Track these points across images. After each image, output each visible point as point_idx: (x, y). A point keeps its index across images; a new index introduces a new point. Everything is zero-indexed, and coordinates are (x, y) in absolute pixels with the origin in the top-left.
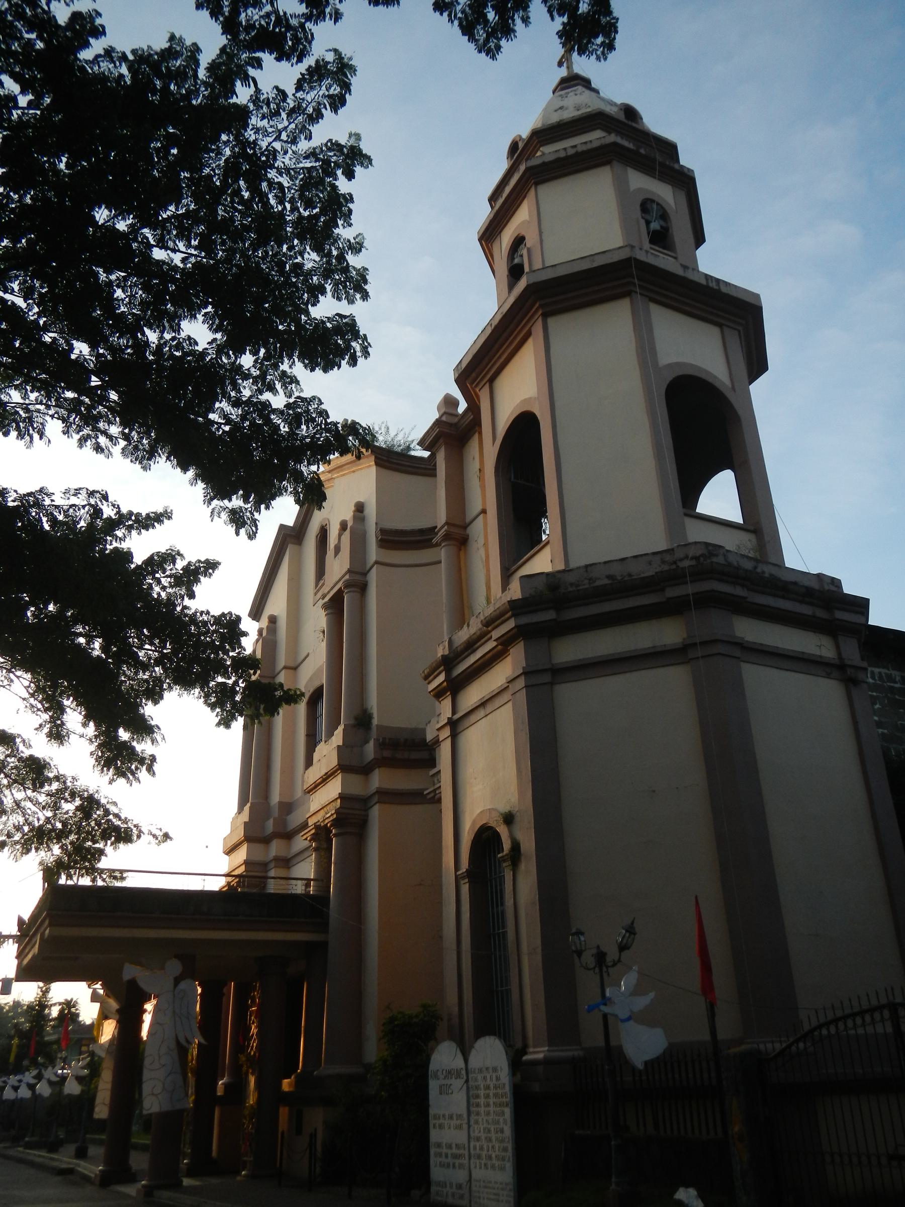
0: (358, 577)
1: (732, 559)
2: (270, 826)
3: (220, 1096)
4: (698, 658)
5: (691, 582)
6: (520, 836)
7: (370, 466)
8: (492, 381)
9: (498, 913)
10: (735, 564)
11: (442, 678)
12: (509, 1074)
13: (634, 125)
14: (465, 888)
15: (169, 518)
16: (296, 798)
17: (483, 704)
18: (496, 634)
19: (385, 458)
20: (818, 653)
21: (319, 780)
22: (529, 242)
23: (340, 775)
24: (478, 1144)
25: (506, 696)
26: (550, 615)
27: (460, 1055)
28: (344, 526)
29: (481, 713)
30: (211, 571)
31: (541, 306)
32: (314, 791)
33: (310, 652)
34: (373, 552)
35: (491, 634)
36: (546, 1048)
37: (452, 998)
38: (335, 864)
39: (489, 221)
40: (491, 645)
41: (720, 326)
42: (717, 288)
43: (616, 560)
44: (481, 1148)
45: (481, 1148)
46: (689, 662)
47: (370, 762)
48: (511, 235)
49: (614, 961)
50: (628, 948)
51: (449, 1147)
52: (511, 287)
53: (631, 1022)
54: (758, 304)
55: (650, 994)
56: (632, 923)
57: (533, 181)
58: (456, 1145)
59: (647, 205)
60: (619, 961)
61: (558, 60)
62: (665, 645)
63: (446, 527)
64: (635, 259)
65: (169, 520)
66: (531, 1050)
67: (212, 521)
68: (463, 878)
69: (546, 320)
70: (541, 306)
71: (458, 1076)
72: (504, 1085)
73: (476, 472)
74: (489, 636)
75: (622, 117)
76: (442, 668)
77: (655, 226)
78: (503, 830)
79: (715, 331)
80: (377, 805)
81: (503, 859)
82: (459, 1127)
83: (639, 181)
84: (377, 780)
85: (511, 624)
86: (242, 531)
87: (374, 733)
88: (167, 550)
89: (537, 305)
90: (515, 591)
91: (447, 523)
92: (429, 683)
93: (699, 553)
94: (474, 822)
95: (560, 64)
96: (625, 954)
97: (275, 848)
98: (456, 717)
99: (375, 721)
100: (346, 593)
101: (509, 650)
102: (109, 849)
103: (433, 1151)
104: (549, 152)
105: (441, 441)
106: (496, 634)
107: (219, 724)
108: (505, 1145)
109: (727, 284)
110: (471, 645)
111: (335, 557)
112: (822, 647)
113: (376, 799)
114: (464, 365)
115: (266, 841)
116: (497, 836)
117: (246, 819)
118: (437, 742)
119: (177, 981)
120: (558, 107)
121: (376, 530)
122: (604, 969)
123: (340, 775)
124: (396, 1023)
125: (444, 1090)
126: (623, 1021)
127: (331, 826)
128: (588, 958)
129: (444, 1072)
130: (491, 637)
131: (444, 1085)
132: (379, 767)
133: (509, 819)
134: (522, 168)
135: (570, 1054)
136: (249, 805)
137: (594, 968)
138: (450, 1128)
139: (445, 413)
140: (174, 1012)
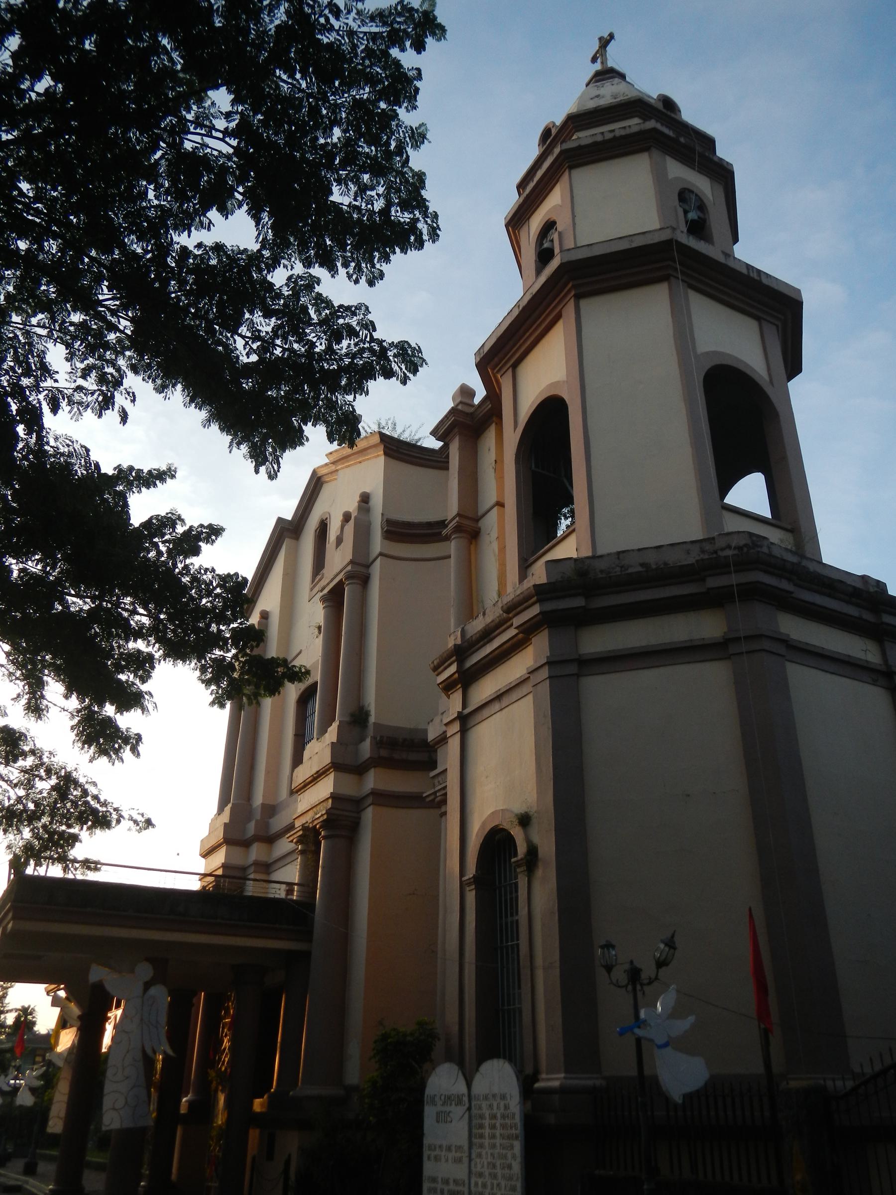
0: (359, 569)
1: (776, 552)
2: (251, 829)
3: (183, 1114)
4: (742, 653)
5: (736, 572)
6: (536, 839)
7: (378, 456)
8: (515, 366)
10: (779, 556)
11: (453, 669)
12: (520, 1103)
13: (673, 115)
14: (471, 897)
15: (173, 477)
16: (281, 800)
17: (499, 697)
18: (517, 621)
19: (395, 448)
20: (863, 657)
21: (310, 779)
22: (560, 226)
23: (333, 773)
24: (480, 1181)
25: (525, 689)
27: (461, 1077)
28: (347, 517)
29: (496, 706)
30: (214, 537)
32: (302, 791)
33: (303, 649)
34: (377, 543)
35: (511, 621)
36: (562, 1075)
37: (452, 1017)
38: (323, 867)
39: (517, 206)
40: (512, 632)
41: (758, 319)
42: (758, 279)
43: (651, 548)
44: (484, 1185)
45: (484, 1185)
46: (729, 658)
47: (365, 762)
48: (542, 220)
49: (650, 978)
50: (667, 965)
51: (446, 1182)
52: (539, 272)
53: (669, 1050)
54: (799, 299)
55: (689, 1018)
56: (673, 936)
58: (454, 1181)
59: (685, 195)
60: (656, 978)
61: (592, 56)
63: (457, 519)
64: (677, 241)
65: (172, 479)
66: (544, 1076)
67: (230, 452)
68: (469, 884)
69: (579, 303)
70: (574, 287)
71: (459, 1102)
72: (514, 1114)
73: (491, 464)
74: (509, 624)
75: (660, 106)
76: (454, 658)
77: (692, 215)
78: (517, 833)
79: (753, 324)
80: (372, 806)
81: (518, 864)
82: (459, 1161)
83: (677, 171)
84: (372, 781)
85: (535, 610)
86: (263, 469)
87: (371, 731)
88: (167, 514)
89: (570, 285)
90: (539, 574)
91: (458, 515)
92: (438, 675)
93: (742, 543)
94: (484, 824)
95: (594, 60)
96: (663, 971)
97: (256, 852)
98: (466, 711)
99: (372, 719)
100: (348, 584)
101: (531, 639)
102: (84, 834)
103: (426, 1186)
104: (584, 137)
105: (456, 430)
106: (517, 621)
107: (213, 703)
108: (513, 1183)
109: (767, 275)
110: (487, 635)
112: (868, 651)
113: (370, 800)
114: (486, 349)
115: (246, 844)
116: (510, 840)
117: (227, 820)
118: (443, 739)
119: (147, 986)
120: (593, 96)
121: (382, 520)
122: (638, 987)
123: (333, 773)
124: (389, 1041)
125: (442, 1117)
126: (661, 1047)
127: (320, 827)
128: (620, 974)
129: (443, 1098)
130: (512, 625)
131: (442, 1112)
132: (375, 767)
133: (524, 820)
134: (557, 151)
135: (590, 1083)
136: (230, 806)
137: (626, 986)
138: (447, 1160)
139: (461, 402)
140: (142, 1020)
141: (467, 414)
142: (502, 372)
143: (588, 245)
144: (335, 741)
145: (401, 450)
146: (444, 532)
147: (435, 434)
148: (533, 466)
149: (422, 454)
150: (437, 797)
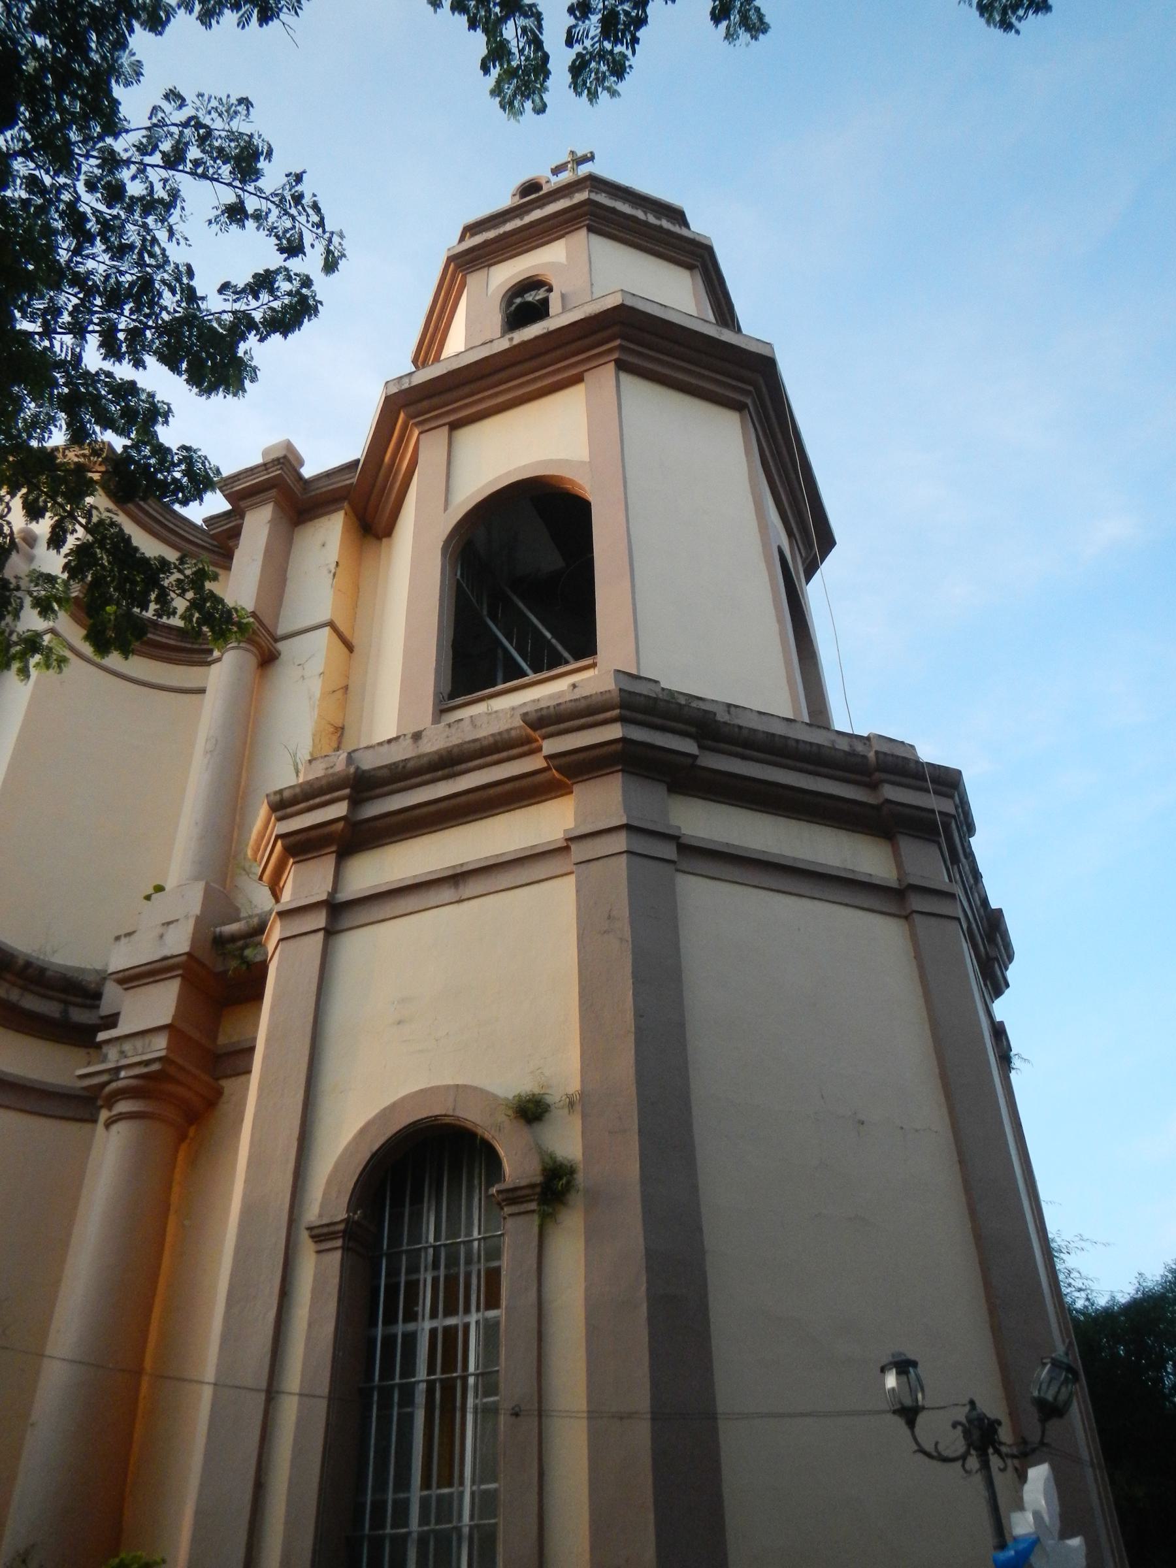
8: (454, 426)
9: (389, 1341)
17: (457, 878)
18: (551, 746)
26: (688, 746)
29: (447, 894)
31: (621, 348)
46: (906, 918)
48: (528, 269)
57: (587, 222)
70: (621, 348)
76: (347, 791)
85: (614, 732)
92: (279, 819)
105: (273, 492)
106: (551, 746)
137: (963, 1458)
143: (661, 305)
147: (226, 485)
148: (459, 573)
150: (118, 1079)
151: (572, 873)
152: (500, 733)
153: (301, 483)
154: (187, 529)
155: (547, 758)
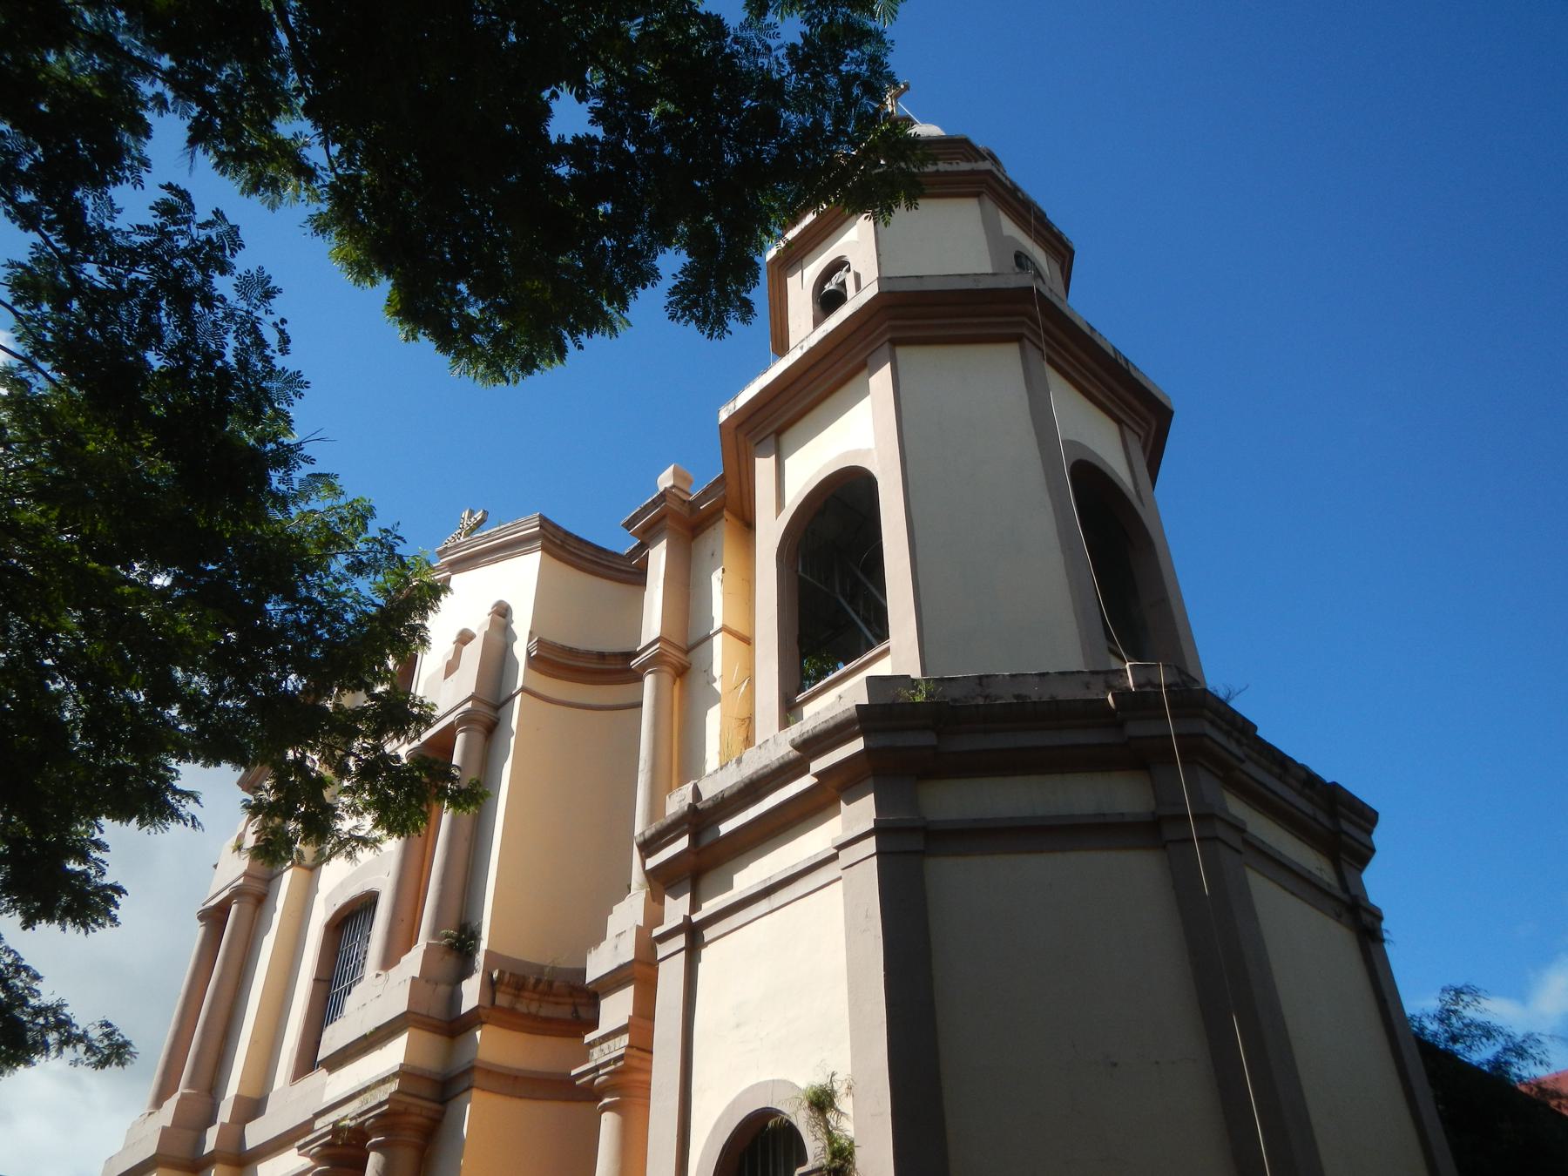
8: (779, 433)
11: (683, 843)
18: (818, 765)
19: (558, 542)
26: (928, 739)
28: (465, 638)
40: (806, 782)
46: (1164, 847)
52: (817, 322)
59: (1021, 259)
62: (1122, 814)
76: (686, 827)
83: (1009, 228)
85: (858, 745)
98: (696, 918)
100: (461, 731)
111: (445, 679)
133: (822, 1102)
136: (177, 1096)
141: (685, 501)
142: (757, 440)
144: (418, 976)
145: (568, 547)
146: (634, 663)
148: (800, 569)
149: (596, 557)
151: (840, 878)
152: (782, 757)
153: (686, 504)
154: (619, 561)
155: (816, 775)
